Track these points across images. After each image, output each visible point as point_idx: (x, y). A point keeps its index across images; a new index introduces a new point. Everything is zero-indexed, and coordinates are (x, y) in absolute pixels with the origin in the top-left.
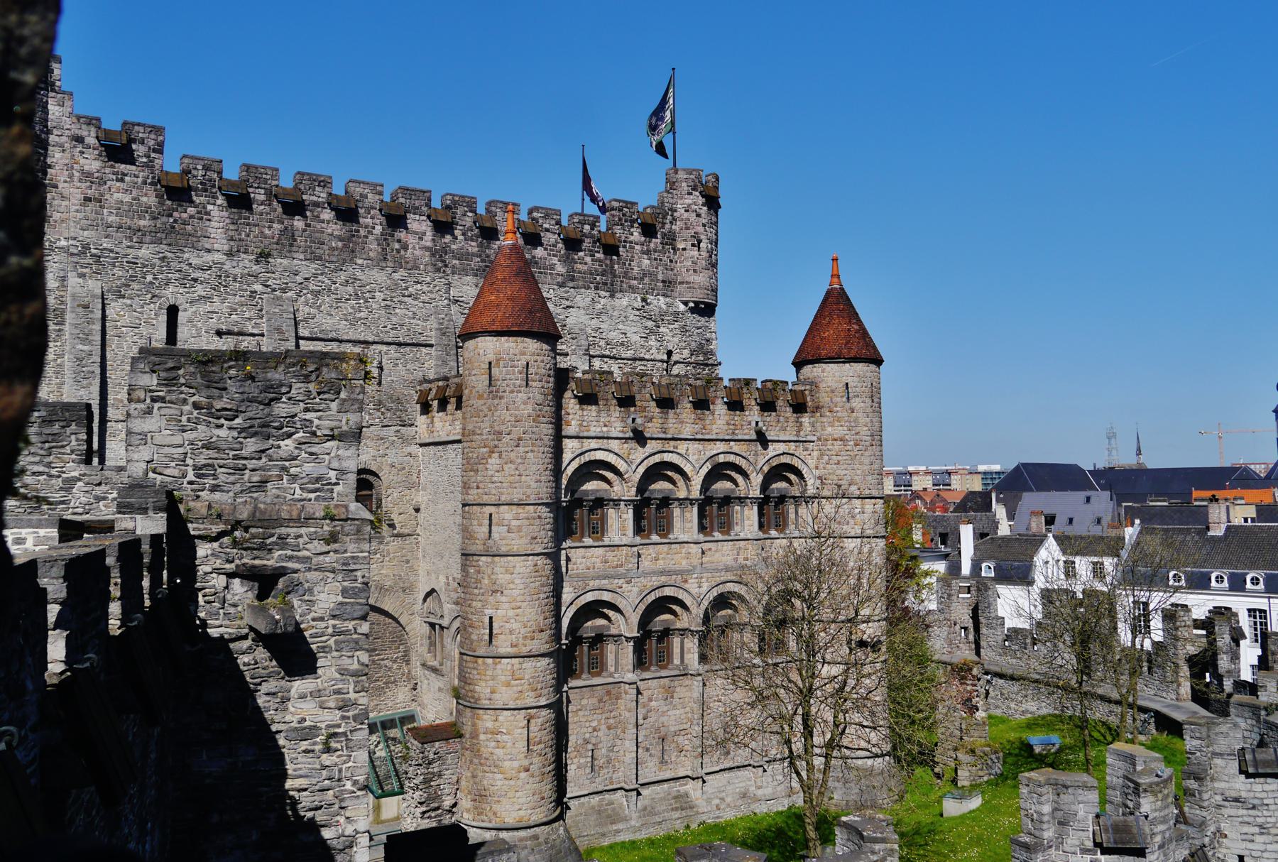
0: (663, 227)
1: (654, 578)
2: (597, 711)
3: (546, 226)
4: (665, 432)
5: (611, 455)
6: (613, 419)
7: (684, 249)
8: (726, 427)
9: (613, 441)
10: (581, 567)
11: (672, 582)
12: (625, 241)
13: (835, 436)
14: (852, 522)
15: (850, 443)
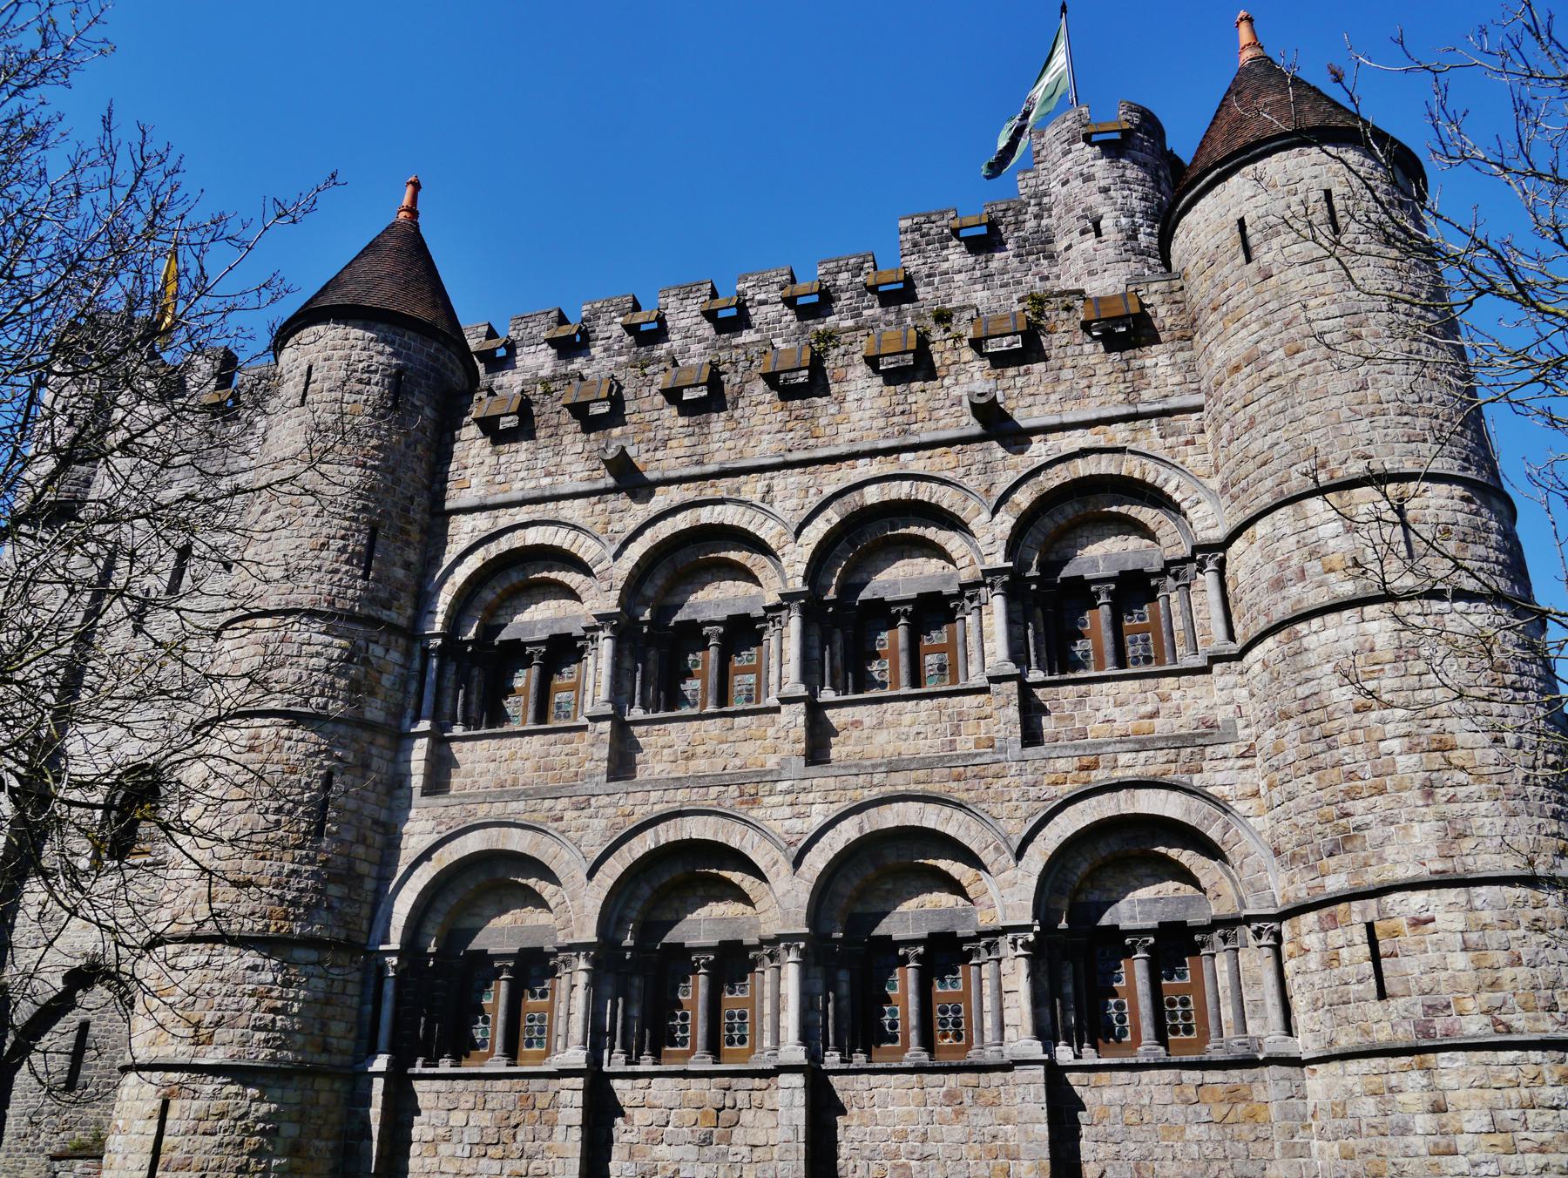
0: (1017, 230)
1: (654, 796)
2: (491, 1151)
3: (762, 297)
4: (698, 463)
5: (563, 532)
6: (566, 459)
7: (1069, 247)
8: (881, 422)
9: (567, 503)
10: (483, 781)
11: (709, 804)
12: (929, 276)
13: (1234, 362)
14: (1314, 567)
15: (1271, 358)
